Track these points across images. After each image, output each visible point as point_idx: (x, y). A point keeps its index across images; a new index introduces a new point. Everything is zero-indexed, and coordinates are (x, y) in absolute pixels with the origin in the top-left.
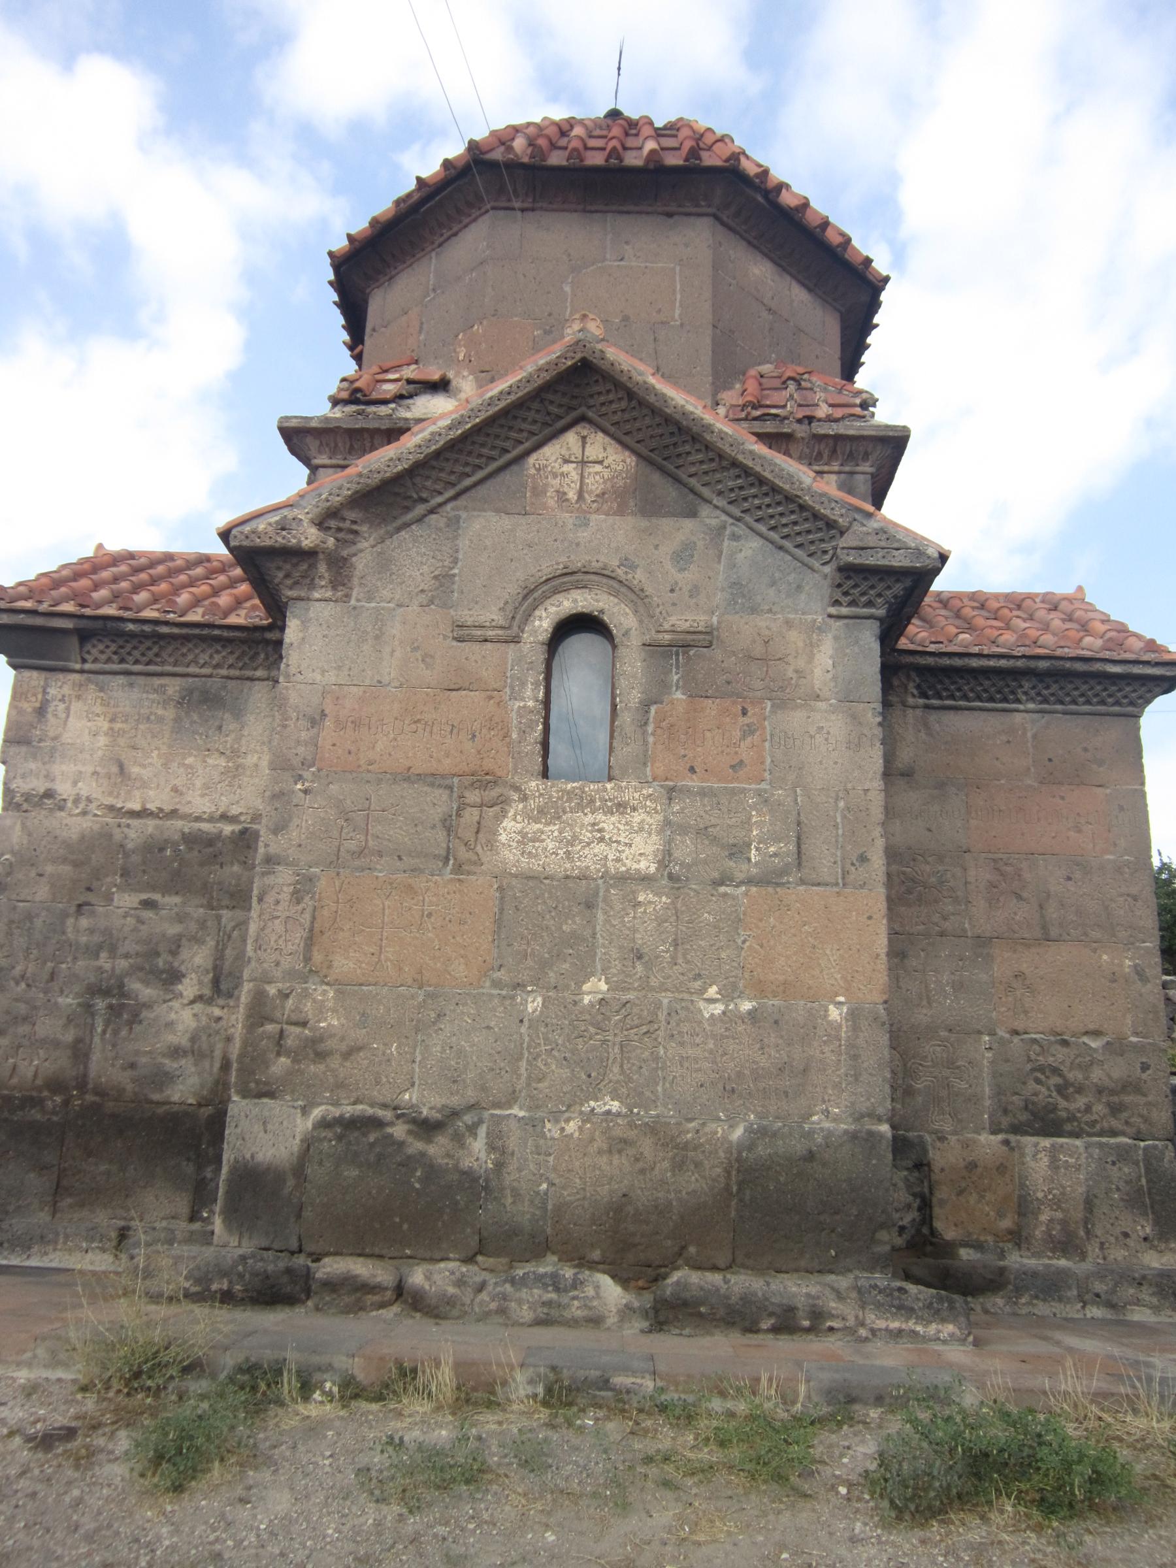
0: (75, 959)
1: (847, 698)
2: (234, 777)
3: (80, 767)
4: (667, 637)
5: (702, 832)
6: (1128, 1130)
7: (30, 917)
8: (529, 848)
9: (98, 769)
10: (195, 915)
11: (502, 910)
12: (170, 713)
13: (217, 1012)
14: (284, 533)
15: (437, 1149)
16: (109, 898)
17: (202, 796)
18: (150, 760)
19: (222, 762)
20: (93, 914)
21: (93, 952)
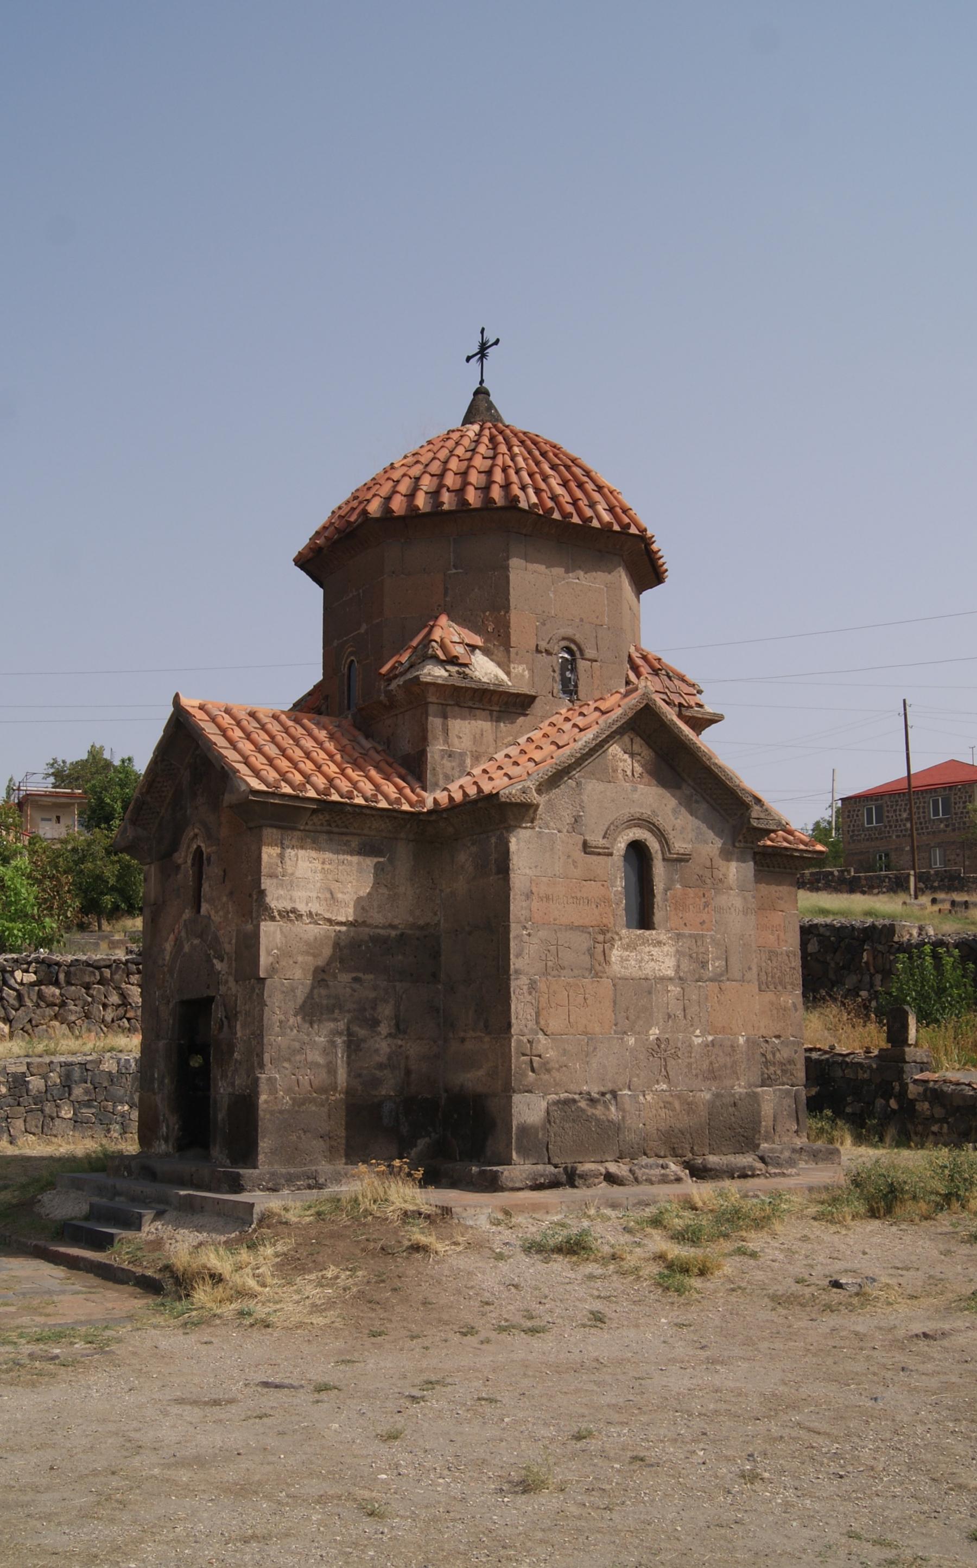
1: (742, 889)
3: (309, 894)
4: (675, 856)
5: (691, 956)
6: (790, 1082)
7: (293, 990)
8: (624, 965)
9: (319, 895)
11: (615, 996)
13: (400, 1042)
14: (524, 795)
15: (598, 1111)
16: (335, 977)
17: (378, 912)
19: (385, 891)
20: (327, 986)
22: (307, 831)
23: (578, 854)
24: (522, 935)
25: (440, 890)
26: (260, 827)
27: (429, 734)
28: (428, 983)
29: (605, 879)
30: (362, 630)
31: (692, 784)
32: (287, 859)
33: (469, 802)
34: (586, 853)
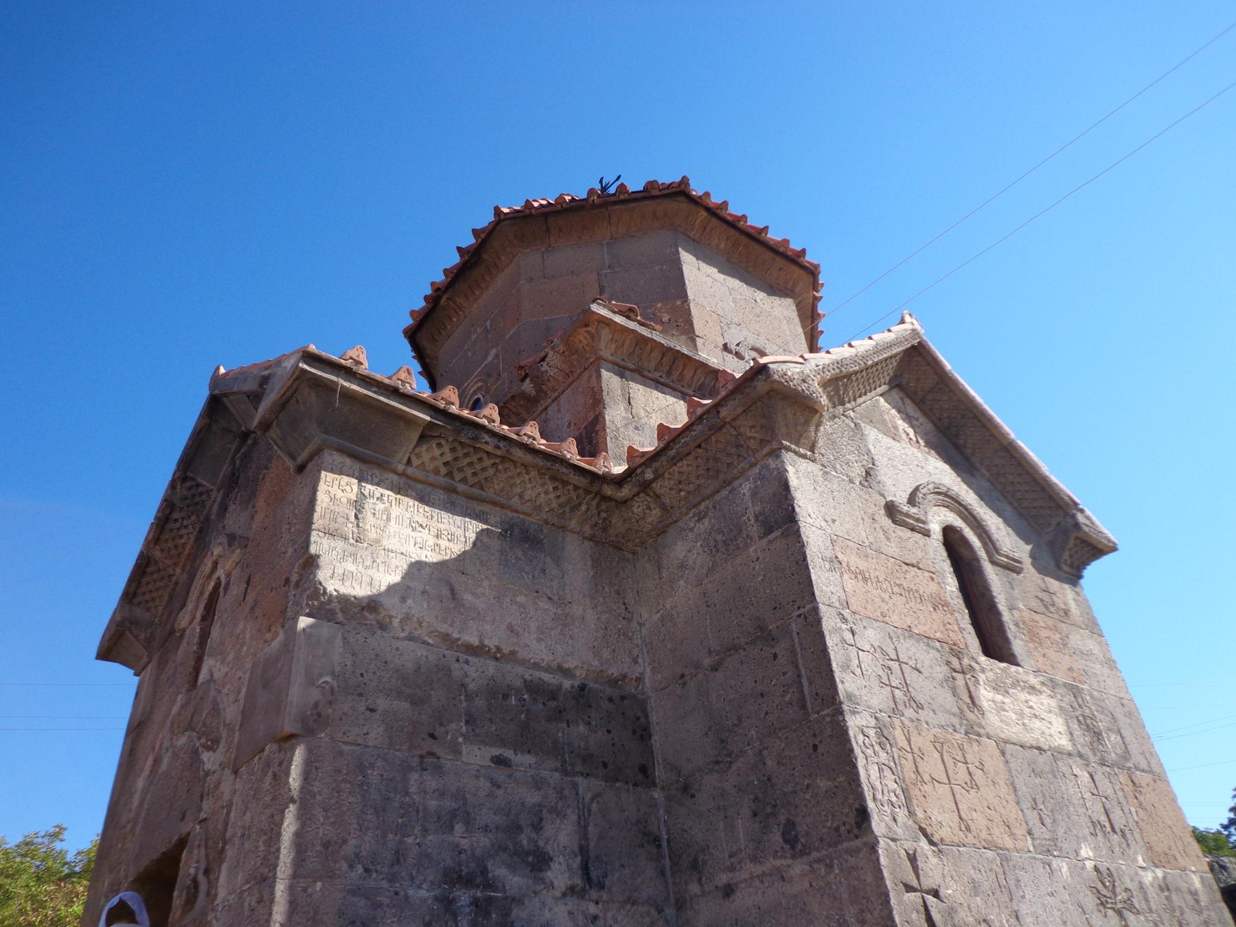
0: (425, 831)
2: (565, 625)
9: (427, 587)
10: (552, 781)
12: (495, 544)
13: (593, 909)
14: (806, 385)
16: (456, 751)
18: (482, 590)
20: (438, 769)
21: (446, 822)
22: (408, 477)
23: (887, 522)
24: (840, 628)
25: (640, 624)
26: (317, 452)
27: (605, 393)
28: (635, 785)
29: (933, 570)
30: (490, 359)
31: (986, 473)
32: (367, 514)
33: (700, 418)
34: (894, 522)
